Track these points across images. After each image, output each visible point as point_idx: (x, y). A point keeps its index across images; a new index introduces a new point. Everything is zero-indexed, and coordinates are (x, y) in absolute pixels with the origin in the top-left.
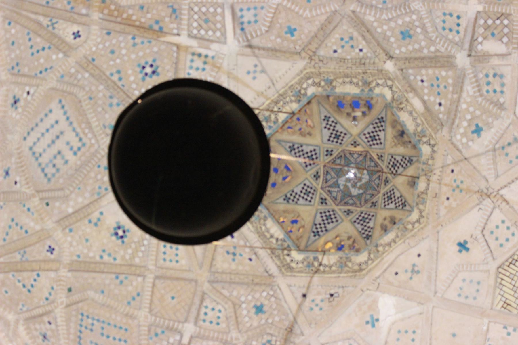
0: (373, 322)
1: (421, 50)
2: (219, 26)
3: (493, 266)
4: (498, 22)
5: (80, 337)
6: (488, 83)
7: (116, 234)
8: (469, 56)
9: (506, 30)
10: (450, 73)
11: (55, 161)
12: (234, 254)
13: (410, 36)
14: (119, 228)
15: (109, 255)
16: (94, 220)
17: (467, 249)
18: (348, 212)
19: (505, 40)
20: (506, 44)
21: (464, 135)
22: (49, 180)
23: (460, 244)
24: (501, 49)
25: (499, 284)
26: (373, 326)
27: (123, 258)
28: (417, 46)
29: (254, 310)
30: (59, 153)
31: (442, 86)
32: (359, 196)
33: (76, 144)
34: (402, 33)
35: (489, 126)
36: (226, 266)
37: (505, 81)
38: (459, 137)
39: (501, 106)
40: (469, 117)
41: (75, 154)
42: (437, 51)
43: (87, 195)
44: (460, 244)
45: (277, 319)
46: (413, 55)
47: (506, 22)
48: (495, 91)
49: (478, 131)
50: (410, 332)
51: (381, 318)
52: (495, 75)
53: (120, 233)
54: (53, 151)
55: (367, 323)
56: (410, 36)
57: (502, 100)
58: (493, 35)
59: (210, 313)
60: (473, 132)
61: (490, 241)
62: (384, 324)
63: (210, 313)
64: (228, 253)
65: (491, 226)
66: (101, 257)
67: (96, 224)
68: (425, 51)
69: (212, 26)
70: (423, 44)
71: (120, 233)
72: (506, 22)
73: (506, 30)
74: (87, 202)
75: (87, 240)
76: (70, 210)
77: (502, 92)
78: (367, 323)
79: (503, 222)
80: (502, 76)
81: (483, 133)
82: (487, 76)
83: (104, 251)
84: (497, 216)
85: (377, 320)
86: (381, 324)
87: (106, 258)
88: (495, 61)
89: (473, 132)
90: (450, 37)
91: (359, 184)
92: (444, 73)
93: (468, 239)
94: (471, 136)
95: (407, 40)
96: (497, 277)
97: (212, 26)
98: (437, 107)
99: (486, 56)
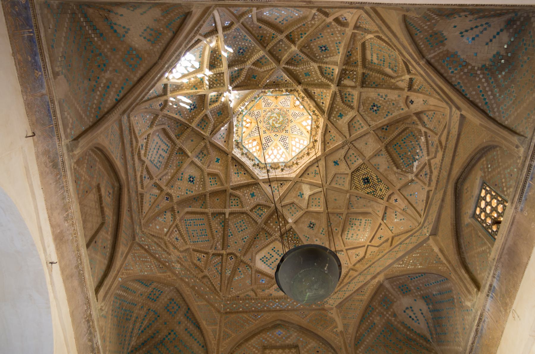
0: (302, 195)
1: (314, 80)
2: (222, 81)
3: (349, 172)
4: (351, 73)
5: (187, 231)
6: (346, 97)
7: (190, 181)
8: (338, 86)
9: (355, 76)
10: (328, 91)
11: (160, 160)
12: (238, 173)
13: (309, 75)
14: (190, 177)
15: (190, 191)
16: (180, 178)
17: (338, 164)
18: (276, 135)
19: (354, 80)
20: (355, 82)
21: (334, 117)
22: (159, 169)
23: (335, 162)
24: (353, 84)
25: (352, 179)
26: (302, 197)
27: (195, 190)
28: (312, 79)
29: (250, 196)
30: (160, 155)
31: (324, 96)
32: (279, 127)
33: (165, 148)
34: (305, 74)
35: (346, 115)
36: (236, 179)
37: (354, 97)
38: (332, 118)
39: (352, 108)
40: (337, 110)
41: (166, 152)
42: (322, 82)
43: (175, 168)
44: (335, 162)
45: (261, 198)
46: (310, 82)
47: (355, 73)
48: (349, 101)
49: (341, 116)
50: (317, 199)
51: (304, 193)
52: (349, 94)
53: (192, 179)
54: (158, 155)
55: (299, 196)
56: (309, 75)
57: (352, 105)
58: (349, 77)
59: (234, 202)
60: (339, 116)
61: (348, 162)
62: (306, 196)
63: (234, 202)
64: (235, 173)
65: (348, 155)
66: (187, 193)
67: (181, 180)
68: (316, 81)
69: (219, 82)
70: (315, 78)
71: (192, 179)
72: (355, 73)
73: (355, 76)
74: (175, 171)
75: (179, 188)
76: (170, 177)
77: (352, 101)
78: (299, 196)
79: (353, 154)
80: (352, 95)
81: (343, 118)
82: (345, 94)
83: (187, 190)
84: (351, 152)
85: (303, 194)
86: (304, 196)
87: (188, 192)
88: (349, 90)
89: (339, 116)
90: (328, 77)
91: (278, 122)
92: (325, 91)
93: (338, 160)
94: (338, 118)
95: (308, 77)
96: (352, 176)
97: (219, 82)
98: (321, 104)
99: (346, 86)
